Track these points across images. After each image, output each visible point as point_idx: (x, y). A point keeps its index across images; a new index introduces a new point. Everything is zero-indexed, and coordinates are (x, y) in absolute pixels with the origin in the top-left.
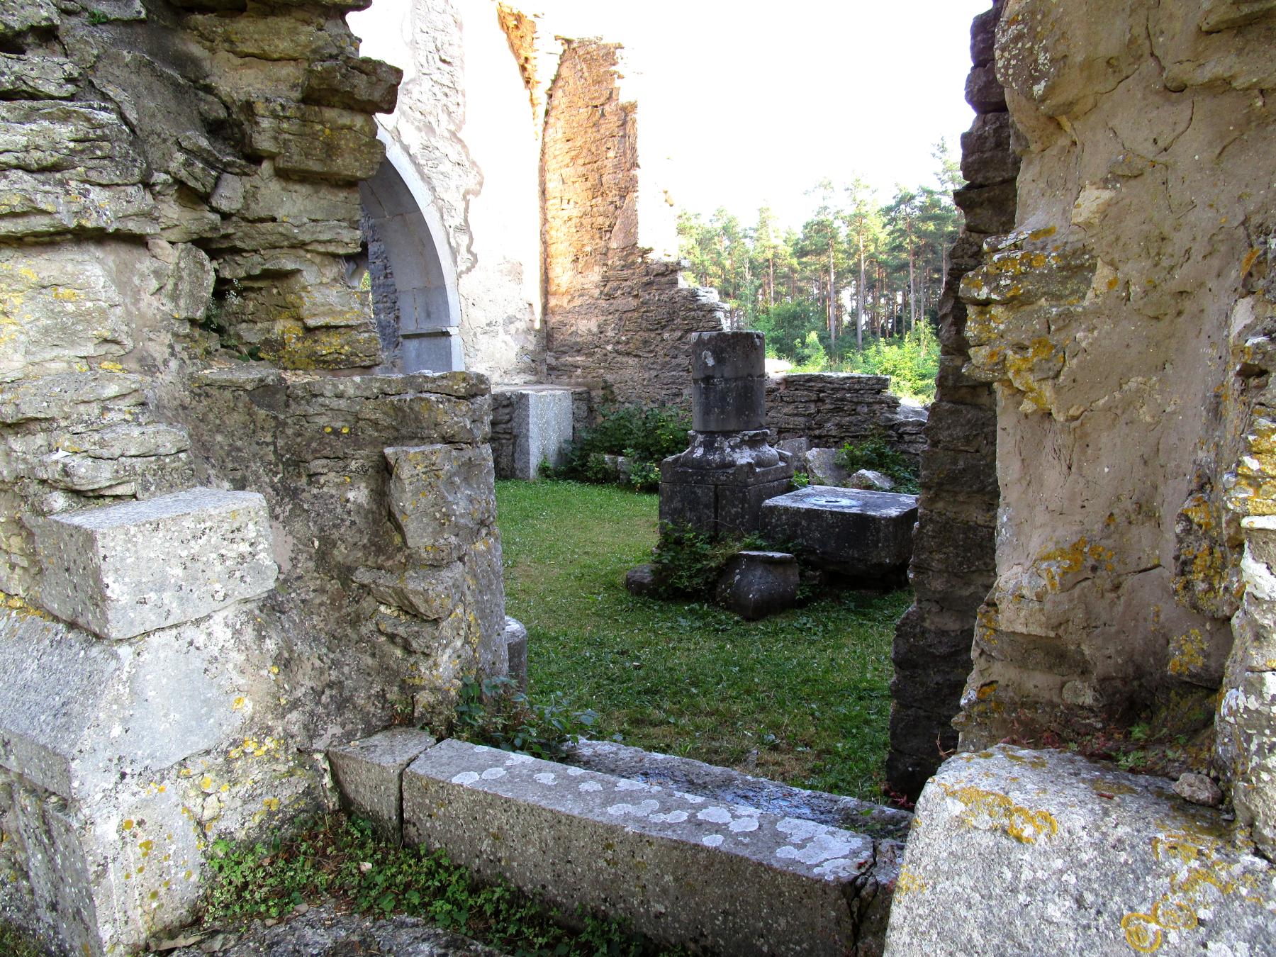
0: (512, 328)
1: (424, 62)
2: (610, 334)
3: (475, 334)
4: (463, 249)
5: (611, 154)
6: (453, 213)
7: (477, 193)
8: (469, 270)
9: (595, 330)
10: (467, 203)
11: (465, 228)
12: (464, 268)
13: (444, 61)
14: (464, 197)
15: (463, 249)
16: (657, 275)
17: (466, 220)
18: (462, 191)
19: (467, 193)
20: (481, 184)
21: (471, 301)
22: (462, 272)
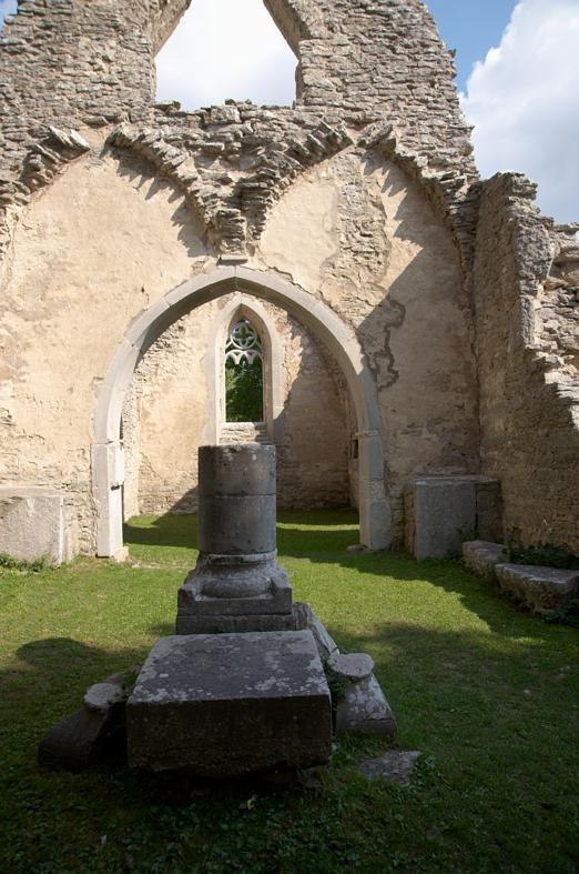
0: (438, 428)
1: (343, 239)
2: (510, 430)
3: (395, 435)
4: (384, 370)
5: (504, 270)
6: (374, 342)
7: (398, 325)
8: (389, 384)
9: (502, 428)
10: (389, 333)
11: (387, 352)
12: (385, 383)
13: (365, 235)
14: (386, 330)
15: (384, 370)
16: (532, 374)
17: (387, 347)
18: (384, 324)
19: (389, 325)
20: (402, 317)
21: (391, 408)
22: (382, 387)
